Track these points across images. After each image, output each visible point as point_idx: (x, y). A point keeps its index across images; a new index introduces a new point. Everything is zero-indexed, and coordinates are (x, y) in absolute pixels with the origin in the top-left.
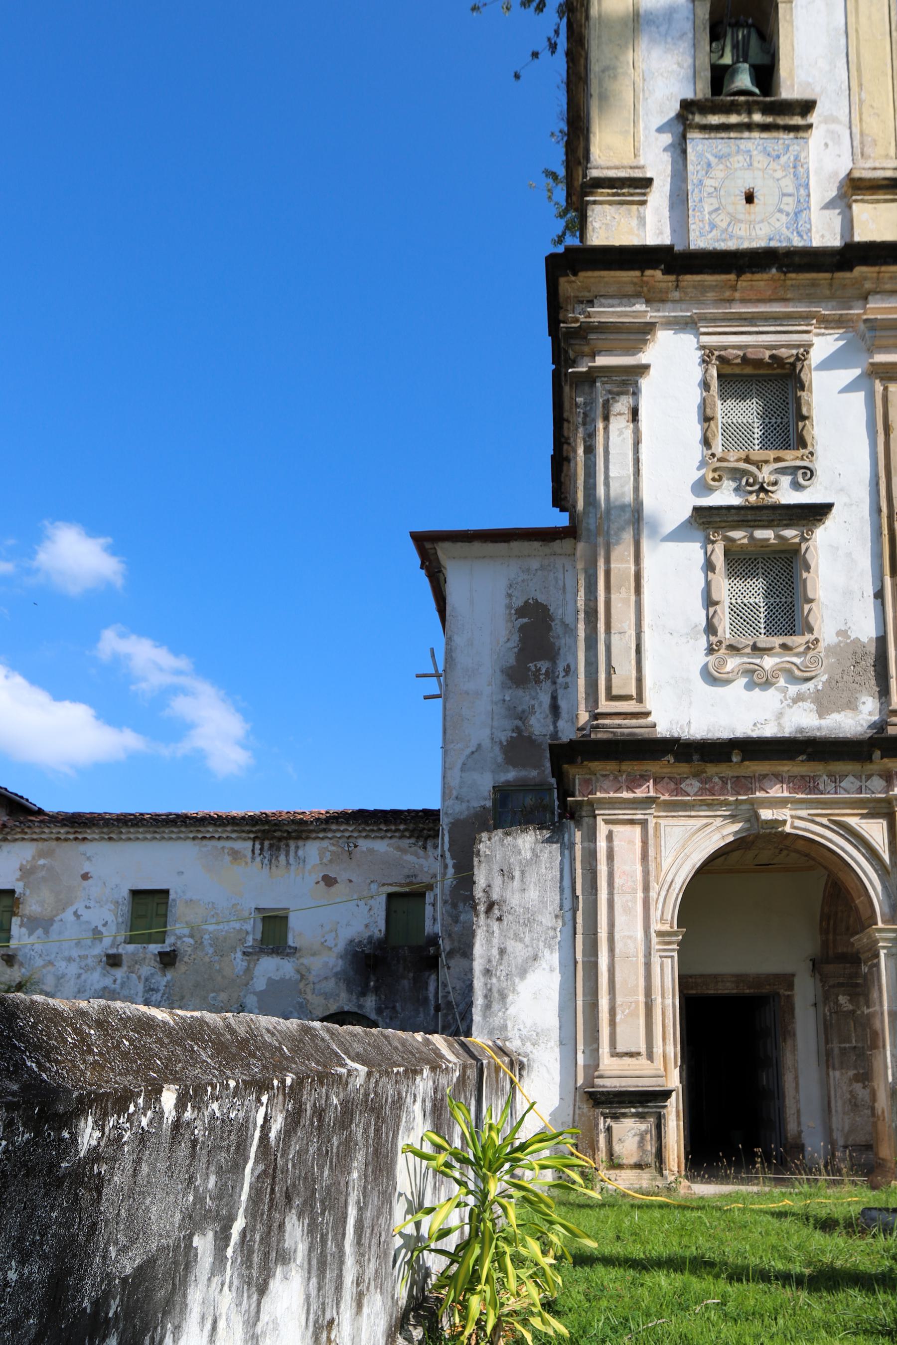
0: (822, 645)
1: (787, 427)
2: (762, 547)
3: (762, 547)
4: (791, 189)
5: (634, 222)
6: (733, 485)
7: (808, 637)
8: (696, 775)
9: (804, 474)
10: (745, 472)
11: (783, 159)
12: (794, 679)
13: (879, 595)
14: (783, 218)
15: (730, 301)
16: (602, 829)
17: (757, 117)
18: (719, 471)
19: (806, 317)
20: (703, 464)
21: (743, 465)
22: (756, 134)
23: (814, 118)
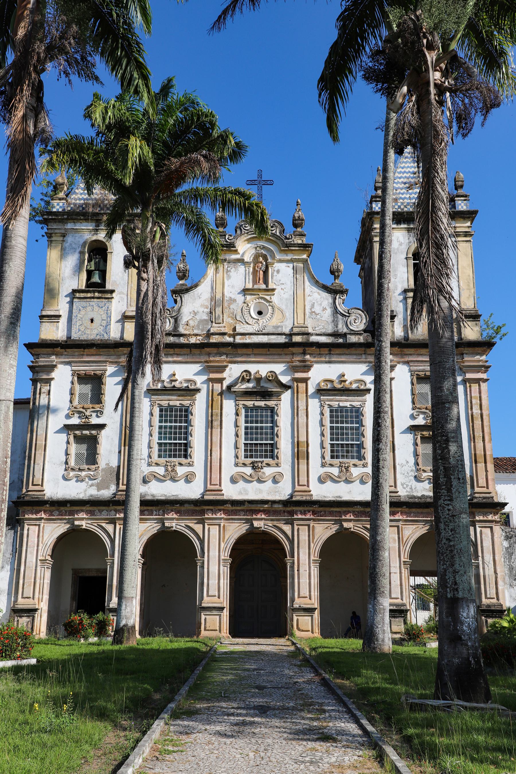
0: (100, 468)
1: (97, 397)
2: (86, 436)
3: (86, 436)
4: (105, 318)
5: (55, 328)
6: (78, 415)
7: (96, 466)
8: (57, 510)
9: (100, 413)
10: (82, 412)
11: (103, 308)
12: (90, 479)
13: (120, 452)
14: (102, 328)
15: (83, 355)
16: (26, 527)
17: (97, 294)
18: (74, 411)
19: (106, 362)
20: (69, 409)
21: (81, 410)
22: (95, 300)
23: (114, 295)
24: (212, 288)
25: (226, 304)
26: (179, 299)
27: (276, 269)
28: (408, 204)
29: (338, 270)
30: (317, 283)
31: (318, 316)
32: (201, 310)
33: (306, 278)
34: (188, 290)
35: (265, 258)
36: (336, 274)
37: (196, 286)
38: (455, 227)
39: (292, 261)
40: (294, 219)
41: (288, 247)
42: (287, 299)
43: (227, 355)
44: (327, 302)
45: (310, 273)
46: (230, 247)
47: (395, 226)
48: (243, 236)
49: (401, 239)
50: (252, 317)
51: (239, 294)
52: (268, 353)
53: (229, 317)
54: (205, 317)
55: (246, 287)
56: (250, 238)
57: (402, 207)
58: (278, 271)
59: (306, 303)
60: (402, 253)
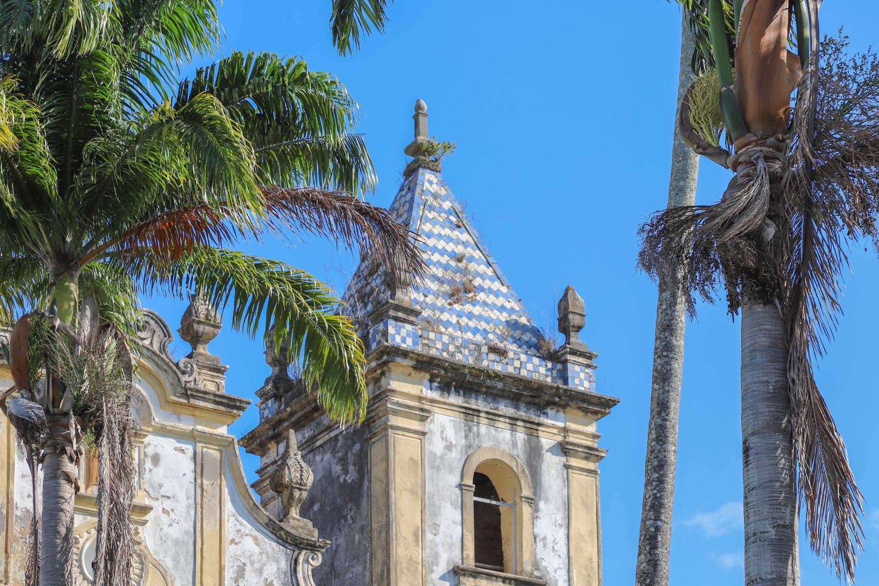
27: (150, 451)
28: (465, 344)
33: (226, 491)
38: (565, 430)
39: (191, 437)
42: (176, 542)
47: (435, 395)
49: (450, 433)
57: (451, 348)
58: (156, 459)
59: (227, 561)
60: (451, 470)
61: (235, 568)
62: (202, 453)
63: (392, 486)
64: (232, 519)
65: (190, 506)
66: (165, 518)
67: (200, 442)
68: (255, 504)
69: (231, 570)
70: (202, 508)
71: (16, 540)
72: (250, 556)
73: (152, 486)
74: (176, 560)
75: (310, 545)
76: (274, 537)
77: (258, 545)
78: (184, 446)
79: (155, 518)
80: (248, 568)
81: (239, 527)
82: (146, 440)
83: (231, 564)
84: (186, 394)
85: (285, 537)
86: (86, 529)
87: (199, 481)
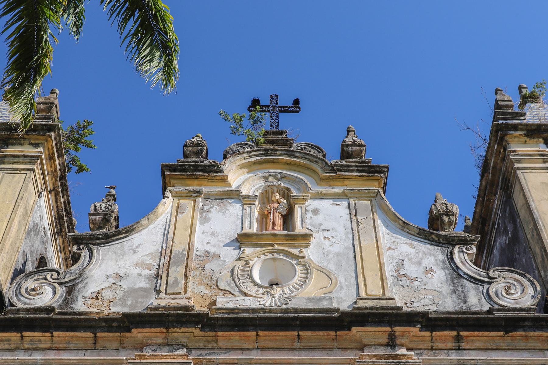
24: (166, 236)
25: (194, 262)
26: (85, 253)
27: (311, 208)
29: (448, 213)
30: (404, 227)
31: (416, 283)
32: (135, 271)
33: (379, 222)
34: (107, 239)
35: (286, 194)
36: (446, 219)
37: (129, 231)
39: (344, 196)
40: (344, 145)
41: (335, 172)
42: (338, 255)
43: (189, 350)
44: (432, 259)
45: (386, 211)
46: (213, 171)
48: (239, 157)
50: (255, 284)
51: (226, 245)
52: (297, 345)
53: (200, 284)
54: (143, 284)
55: (244, 232)
56: (255, 163)
58: (316, 212)
61: (395, 264)
62: (355, 204)
63: (530, 200)
64: (387, 236)
65: (348, 233)
66: (327, 242)
67: (352, 197)
68: (404, 222)
69: (391, 266)
70: (358, 232)
71: (195, 268)
72: (408, 255)
73: (313, 226)
74: (339, 265)
75: (461, 240)
76: (427, 241)
77: (414, 248)
78: (339, 203)
79: (318, 243)
80: (407, 262)
81: (394, 239)
82: (307, 204)
83: (391, 261)
84: (334, 170)
85: (437, 239)
86: (256, 255)
87: (354, 218)
